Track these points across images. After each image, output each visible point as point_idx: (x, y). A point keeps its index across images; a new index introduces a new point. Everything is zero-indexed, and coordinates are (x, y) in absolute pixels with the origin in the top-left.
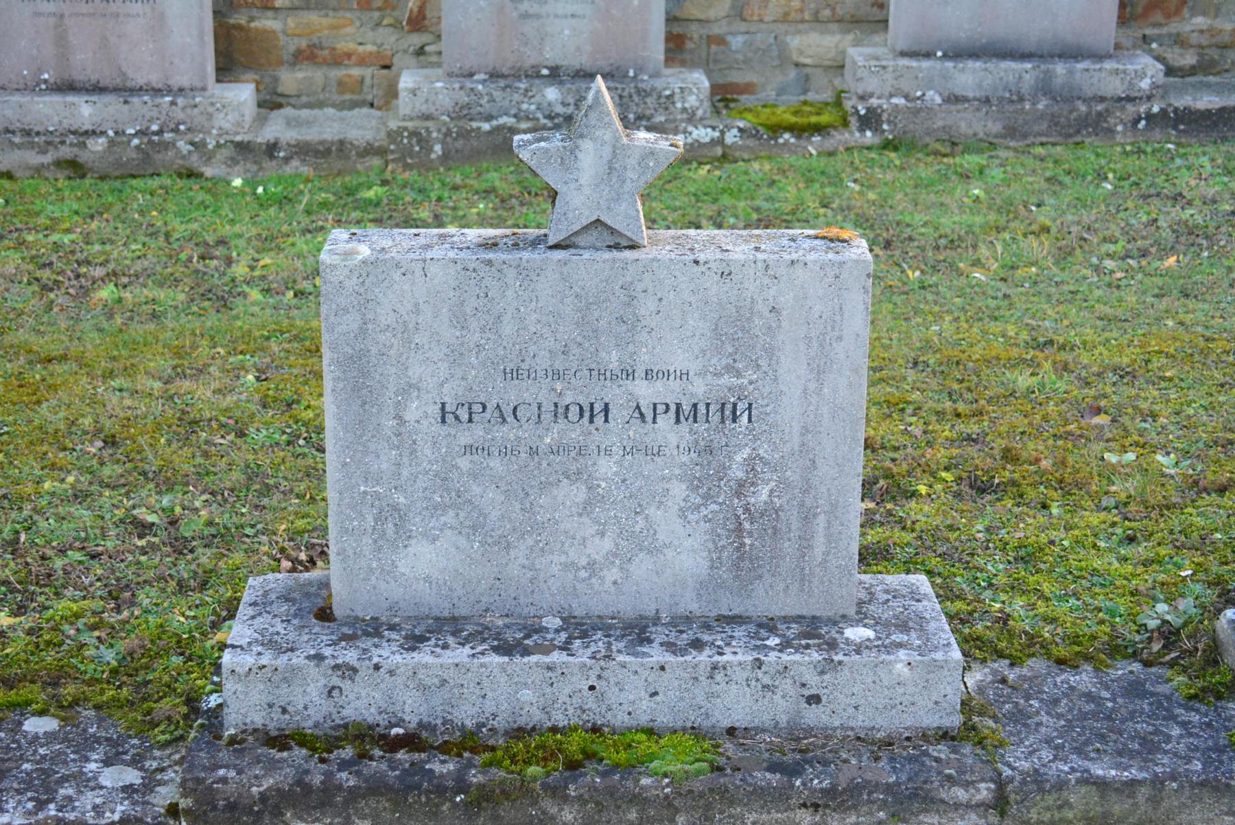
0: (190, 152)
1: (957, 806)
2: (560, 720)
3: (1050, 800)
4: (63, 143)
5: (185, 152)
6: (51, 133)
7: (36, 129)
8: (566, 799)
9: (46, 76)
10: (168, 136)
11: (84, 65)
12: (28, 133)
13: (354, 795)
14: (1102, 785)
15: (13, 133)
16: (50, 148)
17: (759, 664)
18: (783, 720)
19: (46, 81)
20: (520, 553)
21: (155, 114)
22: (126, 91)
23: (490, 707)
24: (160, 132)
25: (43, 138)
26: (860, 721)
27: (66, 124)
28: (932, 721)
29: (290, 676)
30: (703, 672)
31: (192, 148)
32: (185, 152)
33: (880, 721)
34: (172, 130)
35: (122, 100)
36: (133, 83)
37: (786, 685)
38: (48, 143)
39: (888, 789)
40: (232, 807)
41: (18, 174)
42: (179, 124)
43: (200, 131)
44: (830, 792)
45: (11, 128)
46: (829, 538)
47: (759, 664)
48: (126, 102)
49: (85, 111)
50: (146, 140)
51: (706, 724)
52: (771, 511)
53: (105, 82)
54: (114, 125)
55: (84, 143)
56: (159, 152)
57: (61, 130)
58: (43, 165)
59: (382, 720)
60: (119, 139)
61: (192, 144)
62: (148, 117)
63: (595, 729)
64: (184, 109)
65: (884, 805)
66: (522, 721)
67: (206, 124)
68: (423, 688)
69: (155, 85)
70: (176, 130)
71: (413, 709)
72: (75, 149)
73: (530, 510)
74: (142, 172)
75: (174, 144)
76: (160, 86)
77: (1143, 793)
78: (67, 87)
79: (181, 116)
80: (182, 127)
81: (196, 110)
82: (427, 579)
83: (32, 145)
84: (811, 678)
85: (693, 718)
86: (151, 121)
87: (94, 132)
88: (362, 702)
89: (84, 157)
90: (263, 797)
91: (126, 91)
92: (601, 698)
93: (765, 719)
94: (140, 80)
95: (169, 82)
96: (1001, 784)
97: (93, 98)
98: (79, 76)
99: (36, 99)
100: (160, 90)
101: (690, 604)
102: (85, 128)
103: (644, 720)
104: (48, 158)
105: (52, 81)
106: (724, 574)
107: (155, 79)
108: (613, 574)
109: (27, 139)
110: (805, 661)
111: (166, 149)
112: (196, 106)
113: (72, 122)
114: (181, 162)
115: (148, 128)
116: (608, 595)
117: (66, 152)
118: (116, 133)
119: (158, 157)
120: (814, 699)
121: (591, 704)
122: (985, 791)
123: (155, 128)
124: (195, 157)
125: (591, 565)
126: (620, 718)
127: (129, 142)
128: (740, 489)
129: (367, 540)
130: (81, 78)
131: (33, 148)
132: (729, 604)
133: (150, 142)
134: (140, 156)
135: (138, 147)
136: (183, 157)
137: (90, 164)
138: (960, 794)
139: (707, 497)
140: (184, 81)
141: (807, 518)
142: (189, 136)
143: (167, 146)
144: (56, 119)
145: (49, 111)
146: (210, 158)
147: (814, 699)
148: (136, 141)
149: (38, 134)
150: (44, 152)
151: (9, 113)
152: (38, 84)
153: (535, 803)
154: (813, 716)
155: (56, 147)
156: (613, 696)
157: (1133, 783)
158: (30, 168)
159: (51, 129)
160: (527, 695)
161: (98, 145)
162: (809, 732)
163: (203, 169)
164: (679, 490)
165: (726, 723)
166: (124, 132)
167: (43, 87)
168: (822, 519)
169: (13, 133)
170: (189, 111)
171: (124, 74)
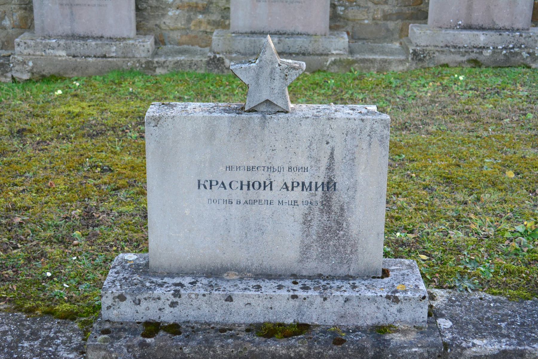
0: (527, 57)
4: (472, 52)
5: (525, 57)
6: (465, 47)
7: (459, 45)
9: (460, 22)
10: (517, 50)
11: (478, 18)
12: (455, 47)
15: (449, 47)
16: (467, 54)
19: (460, 25)
21: (512, 40)
22: (499, 30)
24: (513, 48)
25: (464, 50)
27: (472, 44)
31: (528, 55)
32: (525, 57)
34: (518, 47)
35: (498, 34)
36: (497, 26)
38: (466, 52)
41: (451, 65)
42: (522, 44)
43: (530, 48)
45: (448, 45)
48: (500, 35)
49: (482, 38)
50: (508, 51)
53: (486, 26)
54: (493, 45)
55: (482, 52)
56: (514, 57)
57: (470, 46)
58: (462, 62)
60: (496, 51)
61: (529, 53)
62: (508, 41)
64: (525, 38)
67: (534, 45)
69: (507, 27)
70: (520, 47)
72: (477, 55)
74: (504, 66)
75: (521, 53)
76: (509, 28)
78: (469, 27)
79: (523, 41)
80: (523, 46)
81: (530, 39)
83: (459, 53)
86: (510, 43)
87: (484, 47)
89: (481, 58)
91: (499, 30)
94: (501, 25)
95: (513, 26)
97: (484, 32)
98: (474, 23)
99: (461, 32)
100: (509, 30)
102: (480, 45)
104: (465, 59)
105: (462, 25)
107: (507, 25)
109: (456, 50)
111: (517, 56)
112: (530, 37)
113: (475, 43)
114: (522, 61)
115: (508, 46)
117: (473, 56)
118: (494, 48)
119: (513, 59)
123: (511, 46)
124: (529, 60)
127: (502, 52)
130: (475, 23)
131: (459, 54)
133: (511, 52)
134: (505, 58)
135: (505, 55)
136: (524, 59)
137: (483, 62)
140: (520, 26)
142: (526, 50)
143: (517, 54)
144: (469, 41)
145: (466, 38)
146: (535, 60)
148: (504, 52)
149: (459, 48)
150: (464, 56)
151: (448, 38)
152: (456, 26)
155: (469, 54)
158: (456, 63)
159: (466, 46)
161: (487, 53)
163: (531, 65)
166: (497, 48)
167: (458, 27)
169: (449, 47)
170: (527, 39)
171: (494, 22)
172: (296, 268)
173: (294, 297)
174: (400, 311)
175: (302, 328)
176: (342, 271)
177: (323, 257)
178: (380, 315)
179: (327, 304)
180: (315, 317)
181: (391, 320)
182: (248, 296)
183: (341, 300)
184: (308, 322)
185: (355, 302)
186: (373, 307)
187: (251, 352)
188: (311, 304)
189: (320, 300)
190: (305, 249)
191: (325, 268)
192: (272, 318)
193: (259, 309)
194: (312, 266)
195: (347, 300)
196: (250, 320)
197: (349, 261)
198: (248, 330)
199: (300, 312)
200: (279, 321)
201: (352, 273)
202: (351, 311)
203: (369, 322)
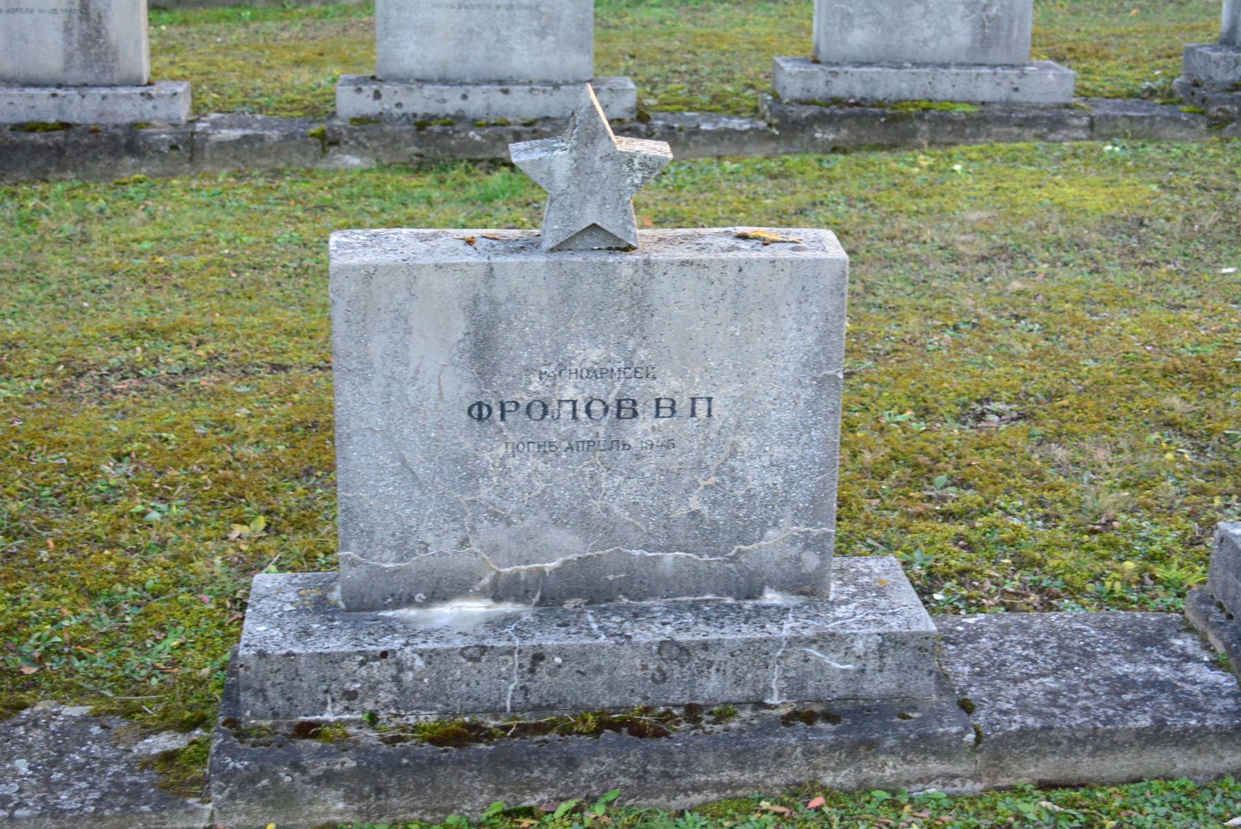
1: (1075, 127)
2: (916, 97)
3: (1111, 124)
8: (924, 121)
13: (842, 117)
14: (1131, 118)
17: (995, 74)
18: (1004, 99)
23: (889, 90)
26: (1034, 99)
28: (1062, 100)
29: (812, 76)
37: (1006, 83)
39: (1048, 118)
40: (794, 123)
44: (1026, 119)
47: (995, 74)
51: (972, 99)
52: (997, 18)
59: (846, 95)
63: (930, 101)
65: (1046, 126)
66: (902, 97)
68: (864, 82)
71: (859, 91)
73: (901, 16)
77: (1147, 122)
82: (860, 46)
84: (1016, 80)
85: (969, 97)
88: (839, 88)
90: (807, 118)
92: (933, 88)
93: (997, 98)
96: (1092, 118)
103: (949, 97)
106: (977, 45)
108: (933, 45)
110: (1013, 73)
116: (930, 52)
120: (1016, 90)
121: (929, 90)
125: (925, 41)
126: (940, 96)
128: (985, 8)
129: (837, 28)
132: (979, 58)
138: (1076, 121)
139: (972, 12)
141: (1011, 21)
147: (1016, 90)
154: (1016, 97)
157: (1143, 118)
160: (904, 85)
162: (1014, 104)
164: (961, 8)
165: (981, 99)
172: (61, 77)
173: (54, 95)
174: (155, 107)
175: (65, 126)
176: (106, 79)
177: (87, 65)
178: (136, 112)
179: (86, 102)
180: (75, 115)
181: (147, 117)
182: (10, 96)
183: (99, 98)
184: (69, 120)
185: (111, 99)
186: (129, 103)
187: (12, 142)
188: (71, 102)
189: (78, 98)
190: (69, 58)
191: (89, 77)
192: (33, 117)
193: (22, 109)
194: (76, 75)
195: (104, 97)
196: (14, 120)
197: (111, 69)
198: (12, 130)
199: (61, 112)
200: (42, 120)
201: (115, 81)
202: (109, 109)
203: (128, 120)
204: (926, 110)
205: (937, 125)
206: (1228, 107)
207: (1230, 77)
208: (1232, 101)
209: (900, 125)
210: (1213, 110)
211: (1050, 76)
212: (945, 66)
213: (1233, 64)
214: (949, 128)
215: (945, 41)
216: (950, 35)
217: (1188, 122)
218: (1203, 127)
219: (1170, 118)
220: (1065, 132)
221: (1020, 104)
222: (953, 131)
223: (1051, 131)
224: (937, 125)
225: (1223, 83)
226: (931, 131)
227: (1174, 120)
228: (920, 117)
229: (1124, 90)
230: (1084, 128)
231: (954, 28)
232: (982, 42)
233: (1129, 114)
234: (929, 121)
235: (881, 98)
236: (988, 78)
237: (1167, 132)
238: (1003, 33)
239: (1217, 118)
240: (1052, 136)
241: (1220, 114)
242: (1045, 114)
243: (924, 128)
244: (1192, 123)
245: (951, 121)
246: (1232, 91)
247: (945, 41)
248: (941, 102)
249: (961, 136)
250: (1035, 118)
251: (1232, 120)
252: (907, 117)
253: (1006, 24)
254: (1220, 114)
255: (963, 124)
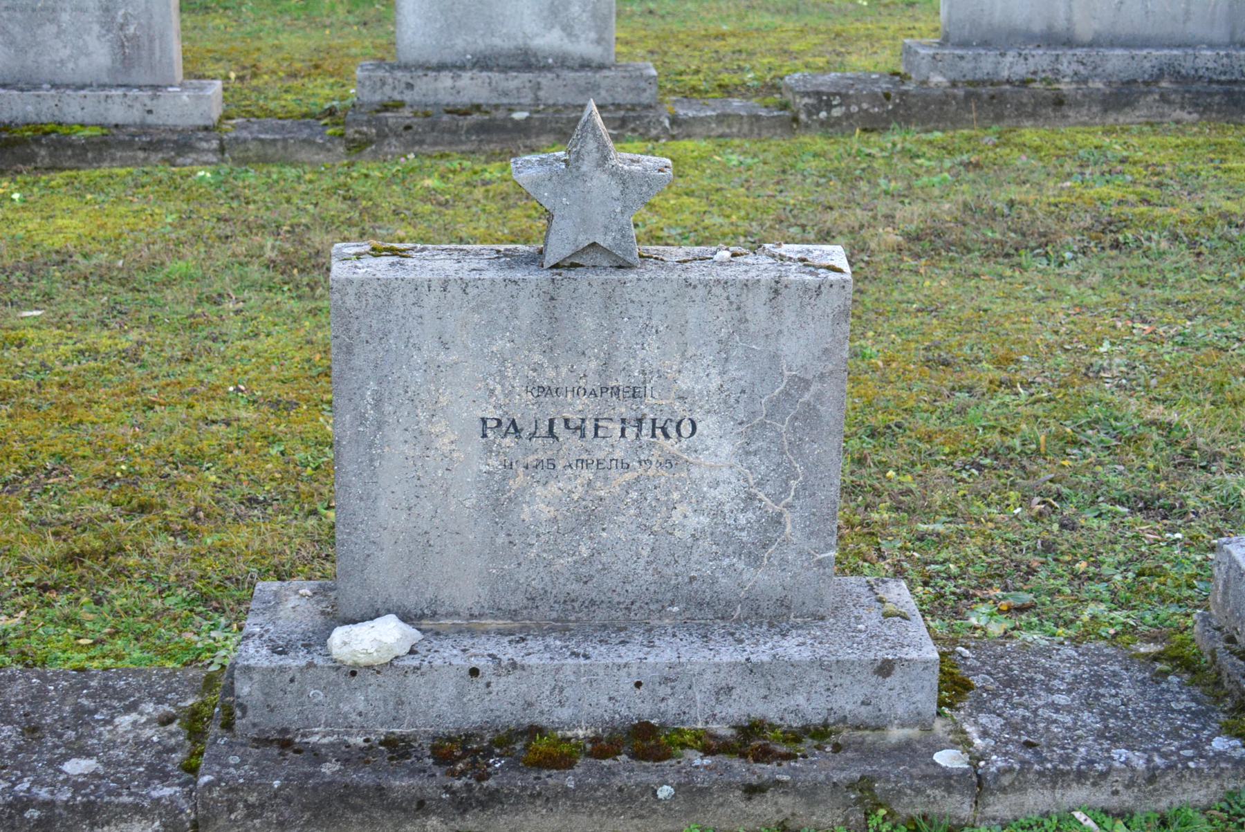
1: (204, 150)
2: (44, 119)
3: (242, 147)
8: (42, 145)
14: (262, 141)
17: (125, 95)
18: (138, 121)
20: (31, 55)
23: (14, 113)
26: (171, 122)
30: (102, 99)
33: (179, 122)
37: (138, 105)
39: (175, 142)
44: (150, 143)
46: (162, 50)
47: (125, 95)
51: (106, 122)
52: (135, 37)
63: (60, 124)
65: (173, 149)
66: (29, 120)
73: (34, 36)
77: (280, 145)
85: (101, 120)
92: (60, 110)
93: (130, 120)
96: (221, 140)
101: (105, 79)
103: (79, 120)
106: (118, 65)
108: (71, 65)
110: (145, 95)
116: (67, 73)
120: (150, 112)
121: (57, 113)
122: (215, 144)
125: (62, 61)
126: (70, 119)
128: (122, 27)
138: (204, 145)
139: (108, 31)
141: (151, 40)
147: (150, 112)
153: (28, 146)
154: (150, 119)
156: (66, 109)
157: (274, 141)
160: (29, 108)
162: (149, 126)
164: (96, 28)
165: (114, 122)
168: (157, 41)
204: (46, 134)
205: (56, 149)
206: (365, 129)
207: (377, 97)
208: (369, 123)
209: (17, 150)
210: (350, 132)
211: (185, 98)
212: (83, 87)
213: (379, 84)
214: (70, 153)
215: (83, 62)
216: (87, 55)
217: (323, 144)
218: (341, 149)
219: (304, 141)
220: (193, 156)
221: (157, 127)
222: (74, 156)
223: (178, 155)
224: (56, 149)
225: (372, 104)
226: (51, 155)
227: (309, 142)
228: (37, 141)
229: (304, 109)
230: (214, 151)
231: (91, 49)
232: (123, 62)
233: (262, 136)
234: (48, 146)
235: (7, 121)
236: (118, 100)
237: (303, 155)
238: (144, 53)
239: (354, 140)
240: (180, 160)
241: (357, 136)
242: (170, 136)
243: (43, 152)
244: (329, 145)
245: (71, 145)
246: (378, 111)
247: (83, 62)
248: (70, 126)
249: (83, 161)
250: (160, 142)
251: (371, 142)
252: (23, 142)
253: (147, 44)
254: (357, 136)
255: (83, 147)
